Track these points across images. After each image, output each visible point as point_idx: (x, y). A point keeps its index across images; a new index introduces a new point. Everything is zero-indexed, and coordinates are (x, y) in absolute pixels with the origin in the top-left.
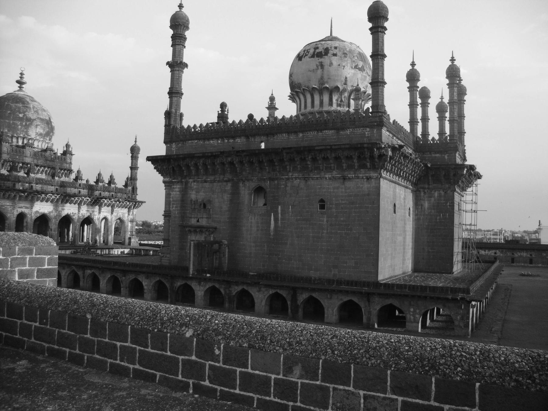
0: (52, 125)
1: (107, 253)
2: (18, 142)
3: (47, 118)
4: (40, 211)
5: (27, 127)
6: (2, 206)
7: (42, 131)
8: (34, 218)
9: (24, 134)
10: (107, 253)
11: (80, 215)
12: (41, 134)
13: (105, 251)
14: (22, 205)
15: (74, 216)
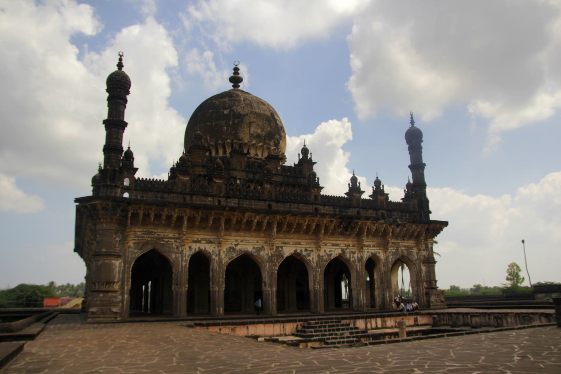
0: (277, 124)
1: (379, 325)
2: (225, 152)
3: (268, 113)
4: (238, 248)
5: (236, 127)
6: (158, 239)
7: (259, 131)
8: (226, 260)
9: (232, 137)
10: (379, 325)
11: (322, 253)
12: (258, 136)
13: (373, 321)
14: (200, 237)
15: (309, 255)
